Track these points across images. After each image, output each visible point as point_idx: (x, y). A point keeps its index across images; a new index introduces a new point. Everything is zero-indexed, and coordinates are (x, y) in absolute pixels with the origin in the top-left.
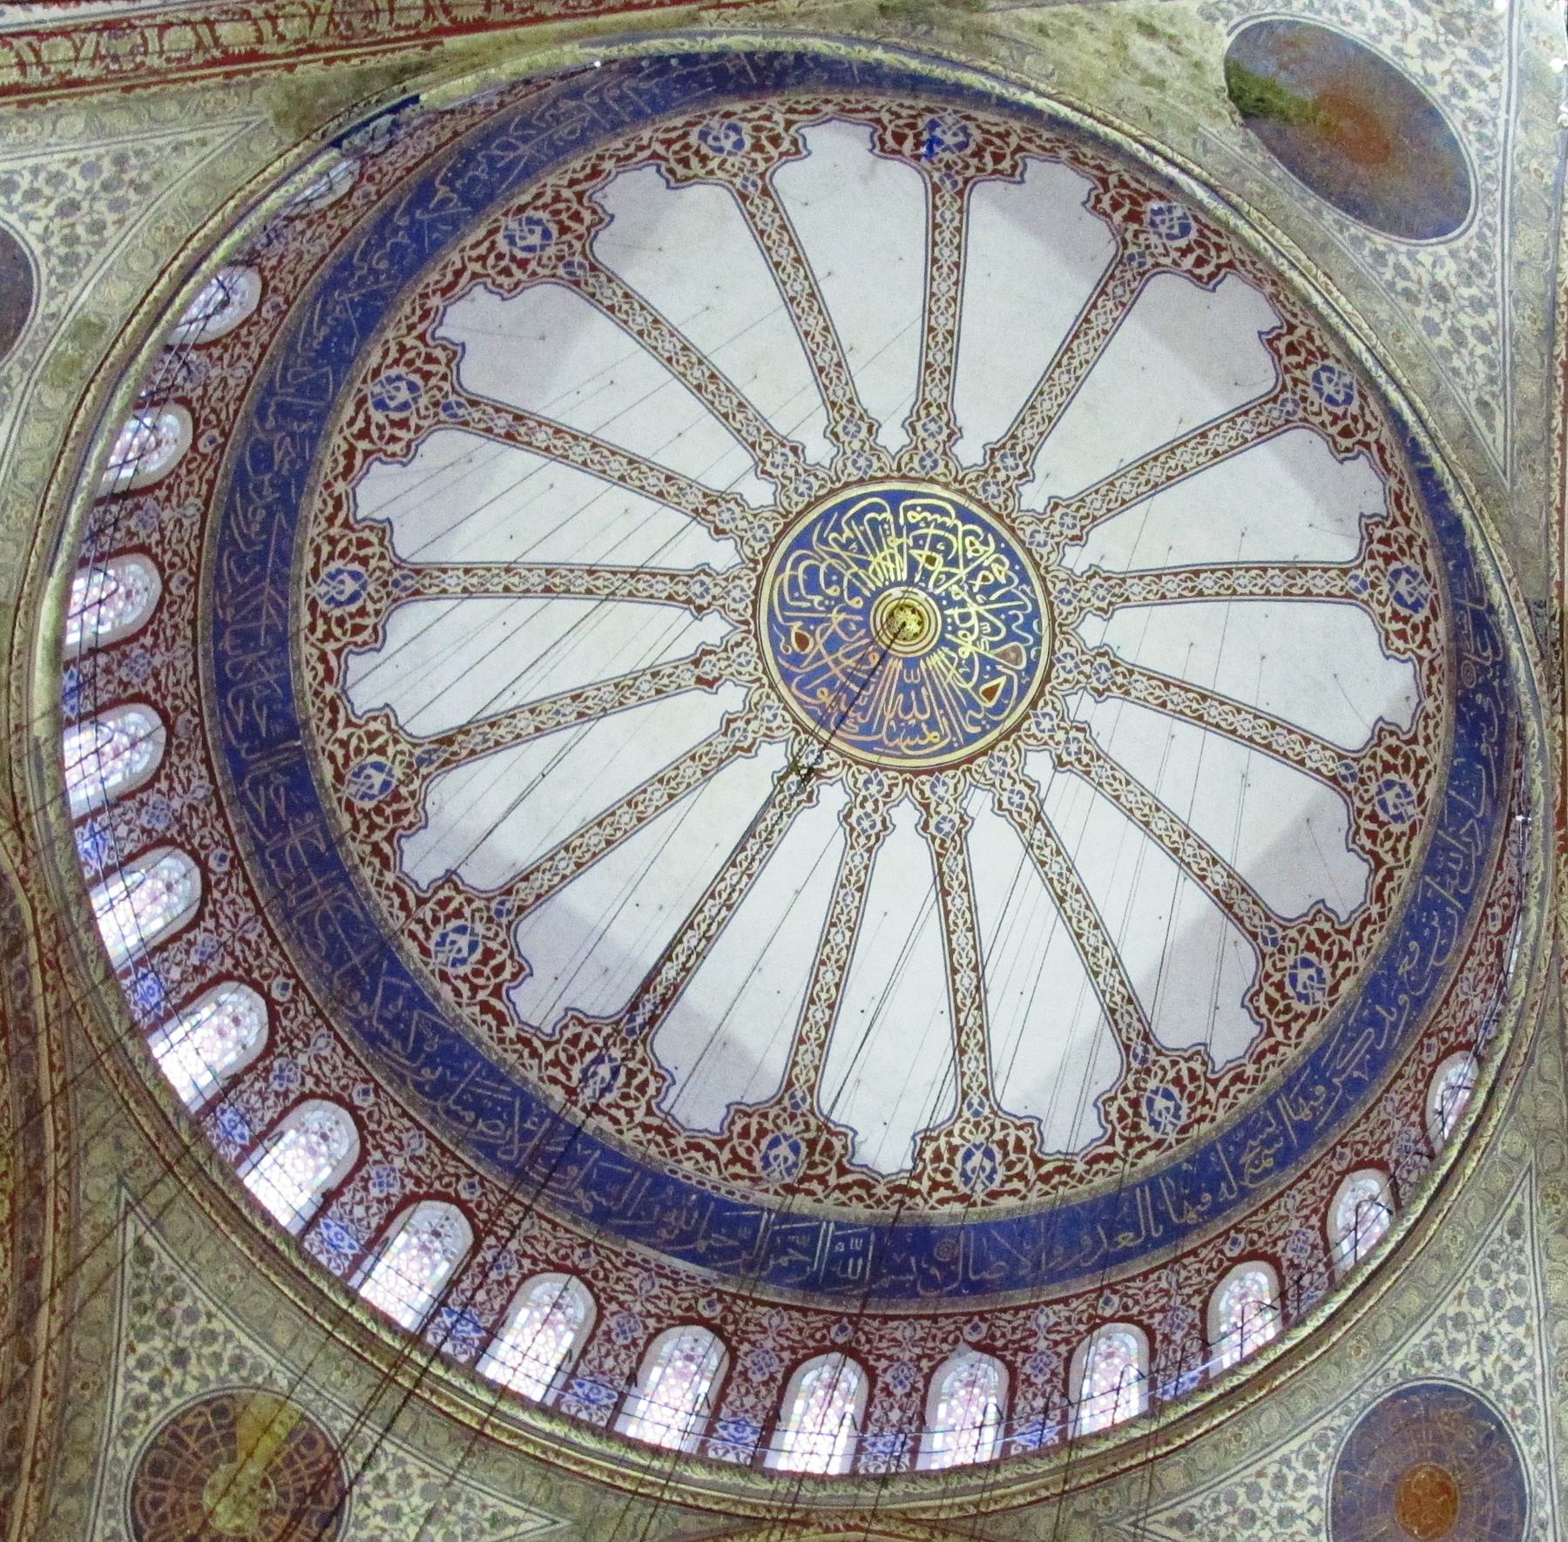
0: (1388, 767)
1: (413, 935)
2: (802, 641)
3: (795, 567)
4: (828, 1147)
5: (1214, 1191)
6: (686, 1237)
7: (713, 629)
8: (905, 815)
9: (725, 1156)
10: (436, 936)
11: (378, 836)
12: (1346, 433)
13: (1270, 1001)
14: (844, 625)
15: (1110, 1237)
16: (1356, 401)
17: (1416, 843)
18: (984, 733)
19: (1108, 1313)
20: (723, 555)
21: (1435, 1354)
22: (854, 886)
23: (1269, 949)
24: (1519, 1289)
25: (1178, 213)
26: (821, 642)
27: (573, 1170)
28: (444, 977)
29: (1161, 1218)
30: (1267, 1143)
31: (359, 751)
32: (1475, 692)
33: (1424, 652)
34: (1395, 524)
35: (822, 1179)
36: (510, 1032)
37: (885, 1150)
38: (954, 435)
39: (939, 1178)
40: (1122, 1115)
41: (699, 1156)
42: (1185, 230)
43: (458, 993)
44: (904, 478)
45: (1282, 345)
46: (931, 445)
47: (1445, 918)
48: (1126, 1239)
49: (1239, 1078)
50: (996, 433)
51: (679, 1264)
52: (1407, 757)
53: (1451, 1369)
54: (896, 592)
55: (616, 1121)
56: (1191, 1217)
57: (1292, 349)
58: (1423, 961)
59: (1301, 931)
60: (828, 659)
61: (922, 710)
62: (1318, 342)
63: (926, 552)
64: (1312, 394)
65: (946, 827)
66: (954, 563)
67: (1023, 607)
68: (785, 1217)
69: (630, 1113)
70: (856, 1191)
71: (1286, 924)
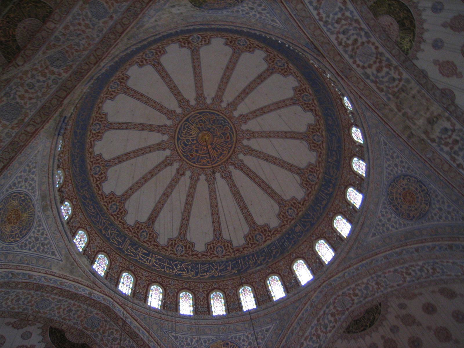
0: (300, 94)
1: (171, 254)
2: (192, 155)
3: (181, 144)
4: (265, 230)
6: (255, 264)
7: (176, 165)
8: (231, 168)
9: (250, 245)
10: (175, 251)
11: (152, 243)
12: (250, 48)
13: (313, 146)
14: (196, 147)
18: (232, 144)
19: (331, 216)
20: (168, 152)
22: (233, 186)
24: (394, 152)
25: (195, 36)
26: (195, 153)
27: (228, 268)
28: (182, 256)
29: (326, 194)
31: (138, 232)
35: (268, 236)
36: (200, 255)
37: (274, 223)
38: (188, 102)
39: (286, 219)
40: (306, 184)
41: (246, 249)
42: (199, 38)
43: (186, 256)
44: (186, 116)
45: (229, 43)
46: (186, 107)
48: (324, 203)
49: (319, 162)
50: (194, 95)
51: (259, 268)
52: (302, 90)
54: (200, 135)
55: (228, 255)
56: (331, 190)
57: (231, 42)
58: (332, 118)
60: (198, 154)
61: (219, 150)
63: (199, 124)
64: (240, 47)
65: (239, 164)
66: (205, 122)
67: (222, 120)
68: (268, 246)
69: (229, 252)
70: (275, 233)
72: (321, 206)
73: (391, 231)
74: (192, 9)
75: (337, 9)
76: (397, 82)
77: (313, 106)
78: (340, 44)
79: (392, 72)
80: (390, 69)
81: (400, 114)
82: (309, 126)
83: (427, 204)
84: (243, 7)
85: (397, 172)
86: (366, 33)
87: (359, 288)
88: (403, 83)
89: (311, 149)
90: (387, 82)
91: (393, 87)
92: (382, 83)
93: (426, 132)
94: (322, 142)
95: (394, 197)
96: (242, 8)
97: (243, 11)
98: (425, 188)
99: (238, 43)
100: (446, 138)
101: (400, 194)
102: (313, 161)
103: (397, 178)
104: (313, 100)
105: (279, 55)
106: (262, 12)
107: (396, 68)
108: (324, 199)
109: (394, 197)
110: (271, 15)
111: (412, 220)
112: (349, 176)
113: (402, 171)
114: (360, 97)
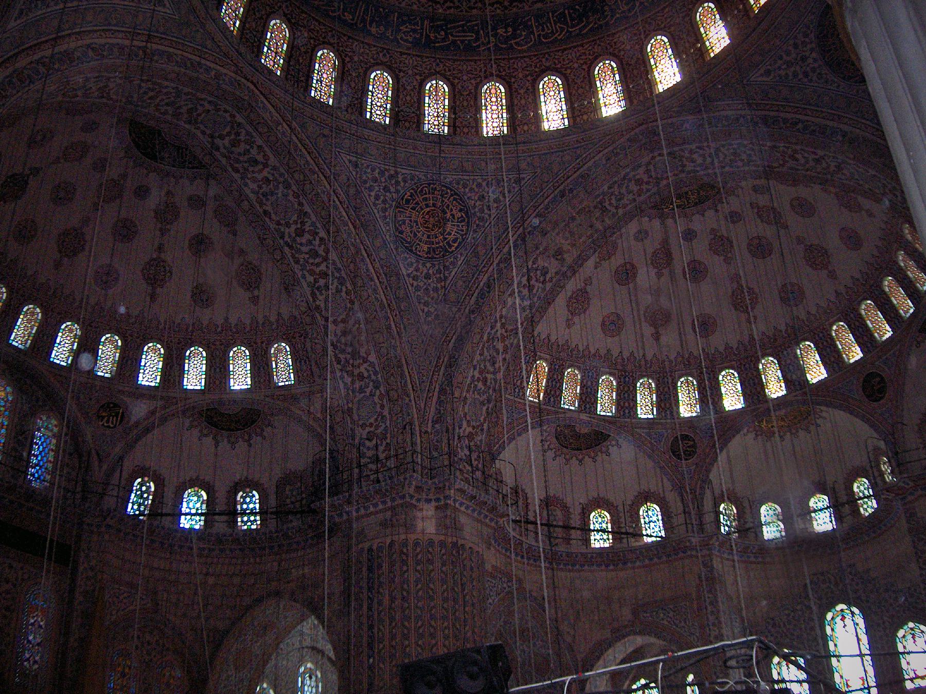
29: (363, 21)
30: (414, 31)
48: (348, 17)
56: (373, 30)
73: (369, 195)
79: (631, 197)
83: (428, 252)
84: (812, 50)
87: (254, 152)
91: (610, 200)
93: (546, 249)
94: (458, 7)
96: (809, 46)
98: (453, 248)
100: (536, 276)
103: (461, 199)
107: (634, 200)
114: (600, 152)
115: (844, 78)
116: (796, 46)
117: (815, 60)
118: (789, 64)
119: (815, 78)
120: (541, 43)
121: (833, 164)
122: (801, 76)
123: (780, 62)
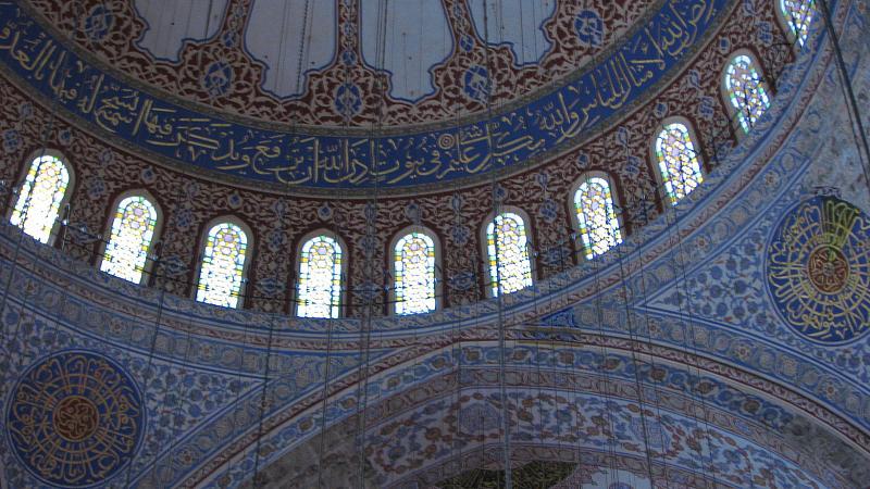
0: (364, 86)
5: (80, 96)
12: (561, 34)
15: (20, 46)
16: (586, 45)
17: (331, 125)
21: (146, 377)
23: (223, 42)
24: (209, 405)
29: (47, 71)
30: (125, 112)
32: (438, 148)
33: (444, 102)
34: (516, 72)
47: (302, 168)
48: (22, 57)
49: (143, 63)
52: (377, 100)
53: (145, 387)
59: (243, 60)
62: (617, 23)
71: (242, 46)
72: (11, 48)
74: (827, 183)
75: (628, 433)
76: (387, 461)
77: (319, 109)
78: (541, 397)
79: (415, 456)
80: (421, 453)
81: (317, 462)
82: (261, 67)
83: (57, 471)
84: (756, 275)
85: (150, 397)
86: (530, 437)
88: (381, 470)
89: (188, 44)
90: (398, 443)
92: (402, 434)
95: (80, 375)
96: (753, 269)
97: (745, 264)
98: (101, 474)
99: (591, 15)
101: (87, 393)
102: (147, 42)
103: (135, 394)
104: (337, 119)
105: (506, 101)
106: (718, 301)
107: (420, 462)
108: (33, 56)
109: (80, 375)
110: (697, 308)
111: (12, 417)
112: (101, 173)
113: (154, 413)
114: (382, 369)
115: (799, 328)
116: (731, 265)
117: (759, 293)
118: (715, 291)
119: (753, 320)
120: (321, 182)
121: (757, 465)
122: (730, 313)
123: (699, 285)
